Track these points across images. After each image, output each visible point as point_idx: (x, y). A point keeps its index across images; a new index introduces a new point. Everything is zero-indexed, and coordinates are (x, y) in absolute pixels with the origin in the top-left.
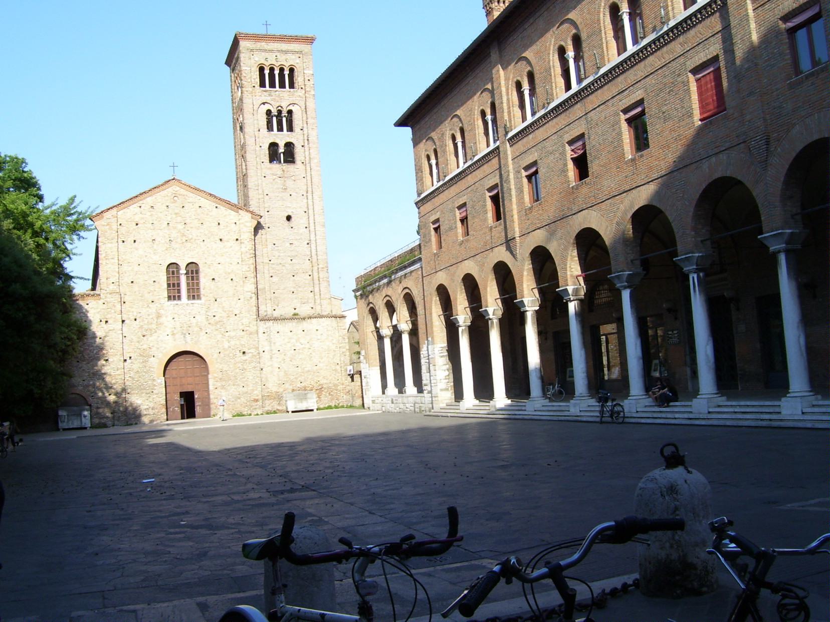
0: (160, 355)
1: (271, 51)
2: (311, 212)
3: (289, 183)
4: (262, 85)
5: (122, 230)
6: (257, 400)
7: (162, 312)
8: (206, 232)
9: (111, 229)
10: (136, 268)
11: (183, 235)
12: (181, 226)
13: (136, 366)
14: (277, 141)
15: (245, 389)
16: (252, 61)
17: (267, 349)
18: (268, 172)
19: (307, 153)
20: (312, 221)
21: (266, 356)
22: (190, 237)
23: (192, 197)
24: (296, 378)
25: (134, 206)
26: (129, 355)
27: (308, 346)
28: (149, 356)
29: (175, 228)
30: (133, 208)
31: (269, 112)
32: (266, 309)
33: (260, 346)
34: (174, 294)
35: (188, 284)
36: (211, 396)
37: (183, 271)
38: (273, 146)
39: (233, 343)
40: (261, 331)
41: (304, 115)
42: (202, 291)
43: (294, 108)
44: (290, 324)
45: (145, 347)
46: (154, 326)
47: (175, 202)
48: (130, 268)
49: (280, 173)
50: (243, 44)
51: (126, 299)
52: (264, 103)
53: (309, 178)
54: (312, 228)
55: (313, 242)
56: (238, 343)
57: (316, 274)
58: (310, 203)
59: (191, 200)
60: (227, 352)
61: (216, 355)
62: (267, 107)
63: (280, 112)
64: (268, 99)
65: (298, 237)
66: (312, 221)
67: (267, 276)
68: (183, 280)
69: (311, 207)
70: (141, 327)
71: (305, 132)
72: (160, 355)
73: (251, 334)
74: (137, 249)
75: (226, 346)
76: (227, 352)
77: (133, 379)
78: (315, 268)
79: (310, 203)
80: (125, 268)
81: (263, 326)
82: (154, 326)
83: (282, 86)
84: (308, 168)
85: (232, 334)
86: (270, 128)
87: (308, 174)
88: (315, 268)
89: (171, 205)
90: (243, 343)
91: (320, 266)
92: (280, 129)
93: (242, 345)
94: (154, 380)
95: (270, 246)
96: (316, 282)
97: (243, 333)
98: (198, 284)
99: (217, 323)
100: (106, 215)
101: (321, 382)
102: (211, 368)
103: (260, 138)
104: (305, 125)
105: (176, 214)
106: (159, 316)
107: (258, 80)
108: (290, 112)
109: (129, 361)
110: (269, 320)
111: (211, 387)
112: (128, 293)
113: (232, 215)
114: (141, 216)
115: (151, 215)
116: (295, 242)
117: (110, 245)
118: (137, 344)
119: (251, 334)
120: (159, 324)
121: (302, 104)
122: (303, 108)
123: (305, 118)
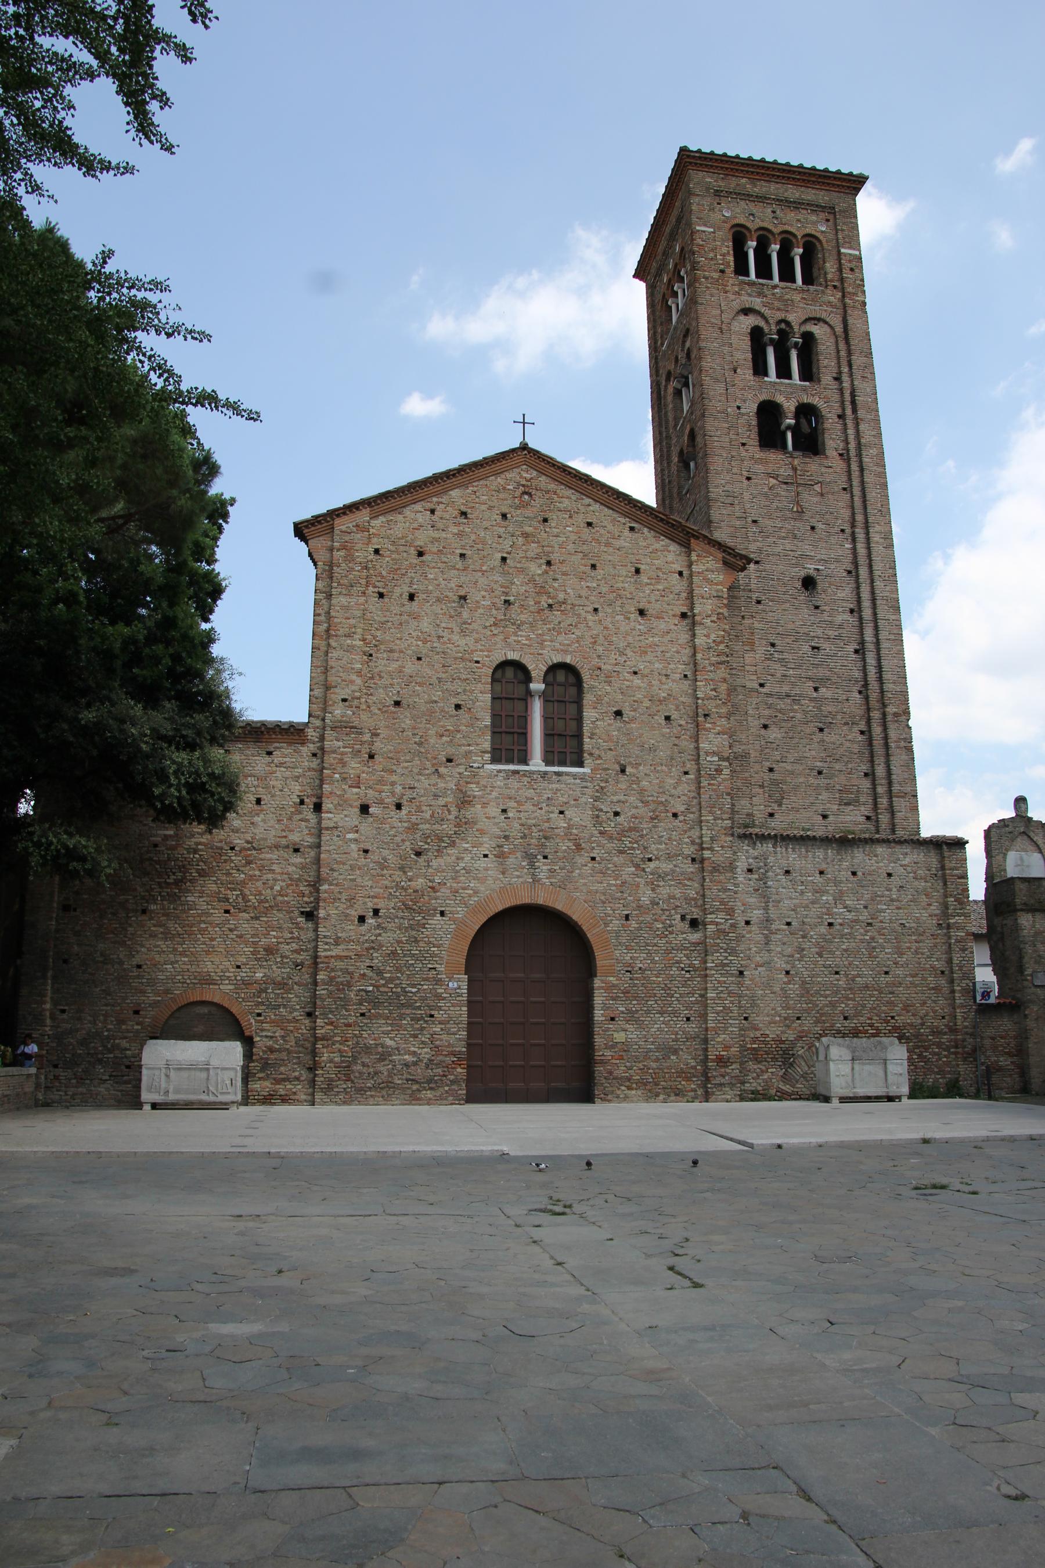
0: (461, 912)
1: (761, 199)
2: (863, 572)
3: (810, 500)
4: (741, 269)
5: (383, 565)
6: (721, 1061)
7: (474, 789)
8: (604, 590)
9: (350, 558)
10: (411, 667)
11: (541, 591)
12: (536, 569)
13: (387, 938)
14: (780, 399)
15: (692, 1028)
16: (716, 217)
17: (756, 915)
18: (760, 468)
19: (851, 432)
20: (865, 595)
21: (755, 934)
22: (561, 596)
23: (568, 498)
24: (833, 1005)
25: (418, 507)
26: (370, 905)
27: (864, 916)
28: (429, 913)
29: (522, 571)
30: (416, 513)
31: (756, 334)
32: (757, 806)
33: (739, 908)
34: (509, 745)
35: (546, 718)
36: (598, 1040)
37: (537, 686)
38: (768, 413)
39: (664, 891)
40: (742, 865)
41: (842, 346)
42: (588, 743)
43: (817, 330)
44: (820, 853)
45: (420, 883)
46: (448, 828)
47: (524, 505)
48: (395, 665)
49: (785, 472)
50: (699, 179)
51: (378, 745)
52: (746, 311)
53: (857, 491)
54: (867, 613)
55: (870, 647)
56: (678, 893)
57: (877, 730)
58: (862, 550)
59: (566, 503)
60: (648, 918)
61: (616, 924)
62: (751, 321)
63: (784, 334)
64: (757, 303)
65: (832, 633)
66: (865, 595)
67: (755, 724)
68: (539, 708)
69: (862, 560)
70: (413, 828)
71: (846, 385)
72: (461, 912)
73: (716, 869)
74: (416, 617)
75: (645, 900)
76: (648, 918)
77: (380, 973)
78: (876, 715)
79: (862, 550)
80: (381, 663)
81: (746, 855)
82: (448, 828)
83: (787, 275)
84: (854, 467)
85: (666, 866)
86: (759, 368)
87: (856, 483)
88: (876, 715)
89: (515, 514)
90: (692, 894)
91: (891, 709)
92: (784, 371)
93: (688, 900)
94: (438, 982)
95: (761, 649)
96: (879, 750)
97: (691, 868)
98: (579, 719)
99: (622, 833)
100: (342, 524)
101: (900, 1020)
102: (601, 962)
103: (733, 392)
104: (845, 370)
105: (526, 535)
106: (464, 801)
107: (731, 259)
108: (809, 338)
109: (371, 921)
110: (763, 838)
111: (599, 1014)
112: (383, 733)
113: (668, 555)
114: (436, 535)
115: (460, 535)
116: (825, 645)
117: (343, 600)
118: (398, 875)
119: (716, 869)
120: (463, 825)
121: (836, 321)
122: (839, 329)
123: (843, 353)
